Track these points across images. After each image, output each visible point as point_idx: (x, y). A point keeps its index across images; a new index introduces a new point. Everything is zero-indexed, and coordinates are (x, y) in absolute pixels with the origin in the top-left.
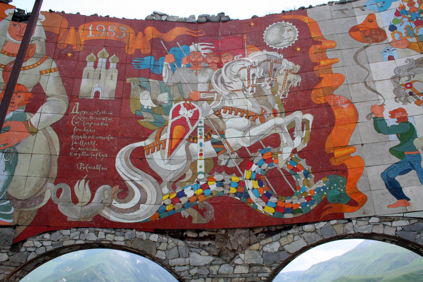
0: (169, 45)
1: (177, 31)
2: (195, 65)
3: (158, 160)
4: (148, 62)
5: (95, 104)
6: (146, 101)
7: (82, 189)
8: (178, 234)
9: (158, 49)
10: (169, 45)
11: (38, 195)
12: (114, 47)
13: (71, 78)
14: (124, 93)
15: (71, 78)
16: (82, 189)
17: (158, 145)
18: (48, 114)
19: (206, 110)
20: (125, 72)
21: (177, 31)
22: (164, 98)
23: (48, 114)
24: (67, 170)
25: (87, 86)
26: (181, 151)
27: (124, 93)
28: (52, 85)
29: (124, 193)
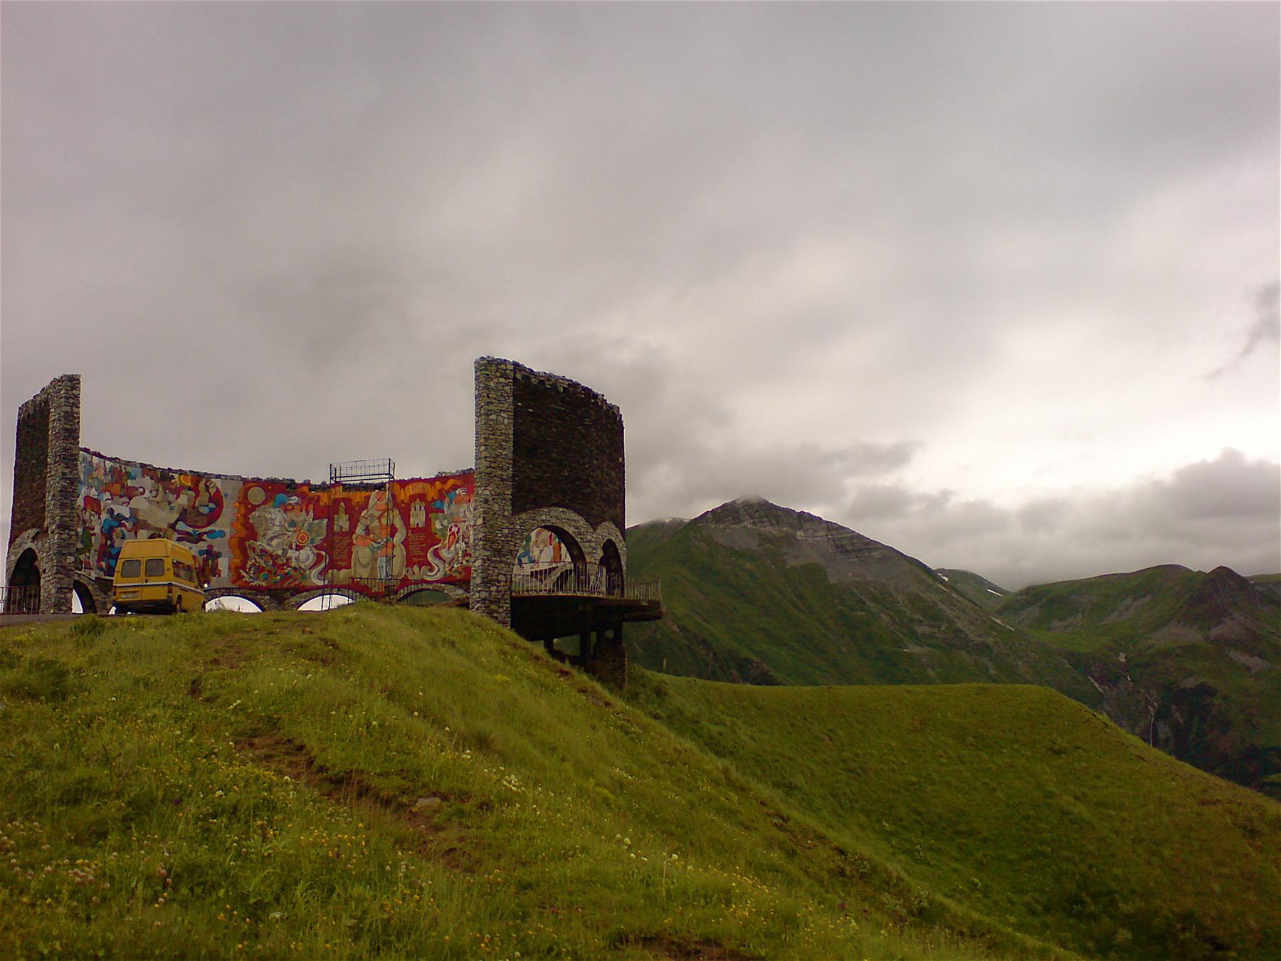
0: (447, 492)
1: (451, 482)
2: (459, 502)
3: (443, 553)
4: (438, 504)
5: (417, 530)
6: (438, 526)
7: (416, 569)
8: (450, 583)
9: (442, 495)
10: (447, 492)
11: (400, 574)
12: (422, 497)
13: (406, 518)
14: (428, 521)
15: (406, 518)
16: (416, 569)
17: (444, 547)
18: (399, 538)
19: (463, 526)
20: (429, 510)
21: (451, 482)
22: (445, 522)
23: (399, 538)
24: (409, 563)
25: (413, 521)
26: (452, 548)
27: (428, 521)
28: (398, 523)
29: (431, 570)
